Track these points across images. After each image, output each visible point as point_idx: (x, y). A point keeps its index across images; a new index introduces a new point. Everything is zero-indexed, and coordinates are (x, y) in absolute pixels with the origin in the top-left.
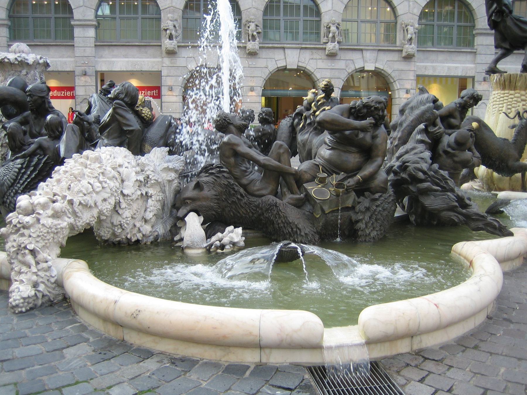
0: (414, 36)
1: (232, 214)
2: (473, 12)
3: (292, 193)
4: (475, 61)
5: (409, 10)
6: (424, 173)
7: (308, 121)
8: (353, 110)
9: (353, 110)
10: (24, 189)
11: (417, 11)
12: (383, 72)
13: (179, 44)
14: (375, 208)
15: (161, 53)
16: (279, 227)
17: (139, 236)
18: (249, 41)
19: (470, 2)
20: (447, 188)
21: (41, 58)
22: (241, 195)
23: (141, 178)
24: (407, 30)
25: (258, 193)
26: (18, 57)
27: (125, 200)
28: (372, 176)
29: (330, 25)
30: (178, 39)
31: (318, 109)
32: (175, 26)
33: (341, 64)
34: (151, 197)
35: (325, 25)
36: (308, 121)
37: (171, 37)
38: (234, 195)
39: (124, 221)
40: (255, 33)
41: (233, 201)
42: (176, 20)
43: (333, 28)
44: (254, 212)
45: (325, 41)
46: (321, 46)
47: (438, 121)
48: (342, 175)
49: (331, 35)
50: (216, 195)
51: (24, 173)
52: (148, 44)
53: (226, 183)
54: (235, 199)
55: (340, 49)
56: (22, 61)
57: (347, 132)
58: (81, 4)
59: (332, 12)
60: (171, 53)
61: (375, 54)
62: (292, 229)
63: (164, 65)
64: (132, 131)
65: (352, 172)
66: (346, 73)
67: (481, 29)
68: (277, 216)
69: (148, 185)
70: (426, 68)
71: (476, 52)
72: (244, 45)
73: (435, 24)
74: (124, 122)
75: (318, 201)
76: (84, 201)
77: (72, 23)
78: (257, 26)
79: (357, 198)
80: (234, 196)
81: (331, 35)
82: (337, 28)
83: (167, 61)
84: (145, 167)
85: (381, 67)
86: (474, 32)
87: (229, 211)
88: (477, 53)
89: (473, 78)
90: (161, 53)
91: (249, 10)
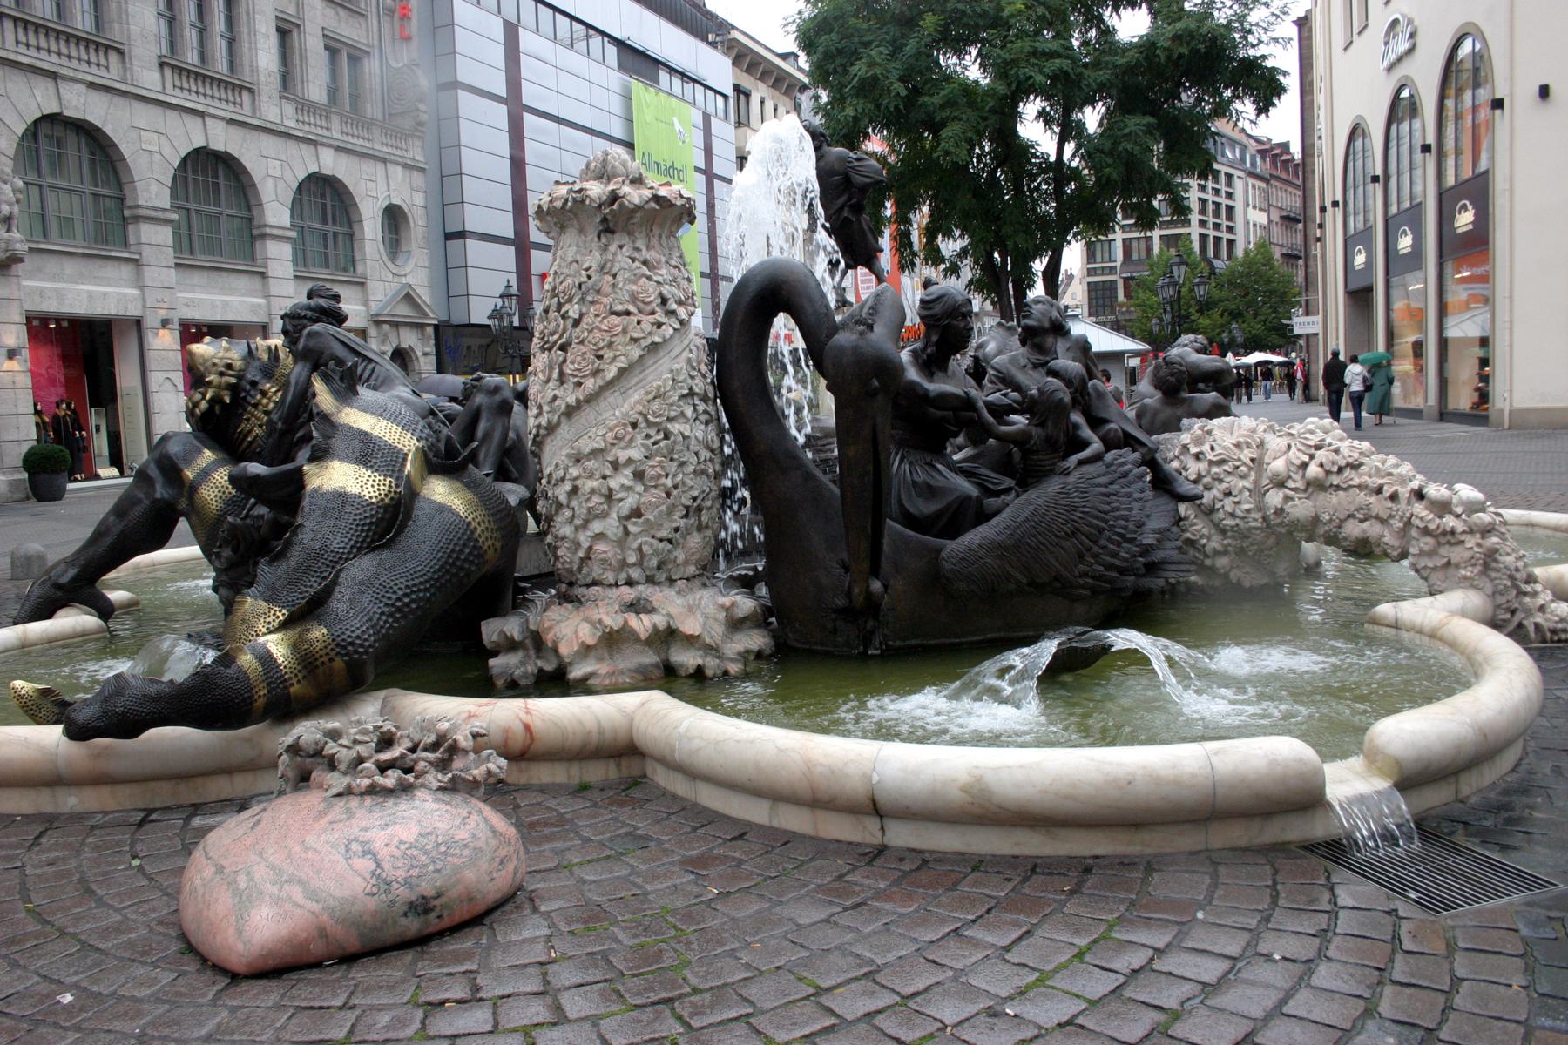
0: (16, 209)
2: (119, 165)
19: (116, 141)
67: (147, 208)
70: (41, 292)
71: (137, 260)
89: (138, 322)
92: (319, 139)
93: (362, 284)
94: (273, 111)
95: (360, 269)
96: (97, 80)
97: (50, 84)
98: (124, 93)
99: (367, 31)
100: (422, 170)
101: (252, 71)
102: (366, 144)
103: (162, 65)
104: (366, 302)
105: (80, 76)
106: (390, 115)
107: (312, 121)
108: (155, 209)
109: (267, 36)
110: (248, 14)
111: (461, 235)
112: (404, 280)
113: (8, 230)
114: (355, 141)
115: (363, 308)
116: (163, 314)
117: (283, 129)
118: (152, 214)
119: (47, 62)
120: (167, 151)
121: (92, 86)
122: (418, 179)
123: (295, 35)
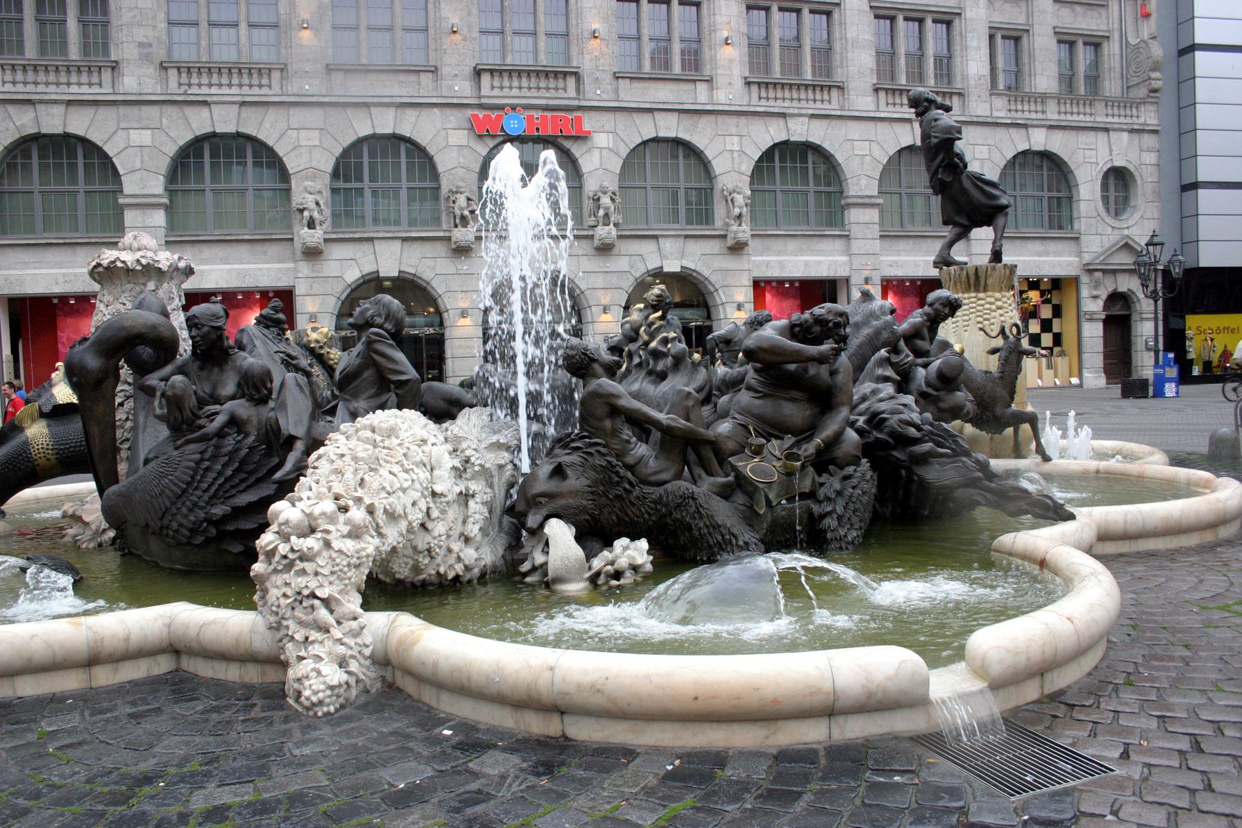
1: (614, 518)
3: (710, 474)
4: (848, 250)
5: (733, 166)
6: (918, 428)
7: (636, 360)
8: (797, 329)
9: (797, 329)
10: (210, 498)
11: (747, 168)
12: (694, 274)
13: (327, 236)
14: (851, 490)
15: (294, 253)
16: (700, 534)
17: (459, 568)
18: (456, 226)
19: (832, 152)
20: (958, 450)
21: (180, 259)
22: (630, 483)
23: (457, 463)
24: (732, 200)
25: (654, 478)
26: (142, 257)
27: (435, 503)
28: (837, 438)
29: (599, 194)
30: (325, 226)
31: (652, 337)
32: (317, 204)
33: (621, 263)
34: (473, 496)
35: (591, 194)
36: (636, 360)
37: (311, 224)
38: (618, 484)
39: (436, 542)
40: (466, 213)
41: (617, 496)
42: (320, 192)
43: (605, 200)
44: (651, 512)
45: (591, 223)
46: (586, 233)
47: (902, 343)
48: (789, 440)
49: (601, 213)
50: (589, 486)
51: (207, 469)
52: (268, 237)
53: (604, 464)
54: (620, 491)
55: (620, 237)
56: (148, 264)
57: (792, 367)
58: (138, 165)
59: (601, 171)
60: (312, 254)
61: (679, 243)
62: (723, 536)
63: (300, 275)
64: (407, 381)
65: (805, 432)
66: (632, 280)
67: (854, 197)
68: (696, 515)
69: (468, 475)
70: (768, 264)
72: (447, 234)
73: (778, 190)
74: (391, 366)
75: (761, 486)
76: (390, 505)
77: (121, 201)
78: (469, 199)
79: (817, 478)
80: (618, 485)
81: (601, 213)
82: (612, 200)
83: (304, 268)
84: (460, 442)
85: (692, 266)
86: (843, 202)
87: (609, 513)
88: (851, 236)
90: (294, 253)
91: (453, 172)
92: (1029, 122)
93: (1077, 239)
94: (979, 107)
95: (1076, 226)
96: (816, 112)
97: (781, 121)
98: (840, 117)
99: (1108, 18)
100: (1155, 132)
101: (963, 78)
102: (1088, 118)
103: (876, 90)
104: (1079, 254)
105: (803, 112)
106: (1128, 88)
107: (1019, 107)
108: (862, 197)
109: (978, 48)
110: (961, 35)
111: (1195, 186)
112: (1126, 232)
113: (740, 225)
114: (1075, 117)
115: (1077, 259)
116: (866, 273)
117: (990, 120)
118: (860, 201)
119: (777, 107)
120: (877, 153)
121: (813, 116)
122: (1150, 141)
123: (1025, 40)
